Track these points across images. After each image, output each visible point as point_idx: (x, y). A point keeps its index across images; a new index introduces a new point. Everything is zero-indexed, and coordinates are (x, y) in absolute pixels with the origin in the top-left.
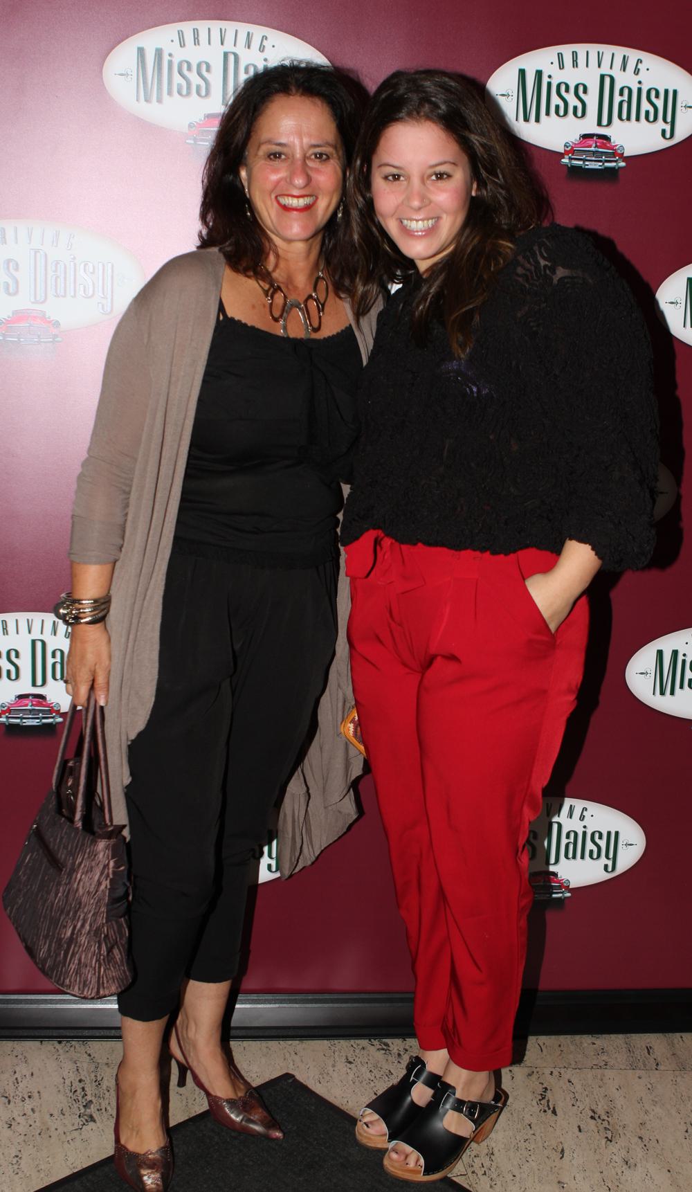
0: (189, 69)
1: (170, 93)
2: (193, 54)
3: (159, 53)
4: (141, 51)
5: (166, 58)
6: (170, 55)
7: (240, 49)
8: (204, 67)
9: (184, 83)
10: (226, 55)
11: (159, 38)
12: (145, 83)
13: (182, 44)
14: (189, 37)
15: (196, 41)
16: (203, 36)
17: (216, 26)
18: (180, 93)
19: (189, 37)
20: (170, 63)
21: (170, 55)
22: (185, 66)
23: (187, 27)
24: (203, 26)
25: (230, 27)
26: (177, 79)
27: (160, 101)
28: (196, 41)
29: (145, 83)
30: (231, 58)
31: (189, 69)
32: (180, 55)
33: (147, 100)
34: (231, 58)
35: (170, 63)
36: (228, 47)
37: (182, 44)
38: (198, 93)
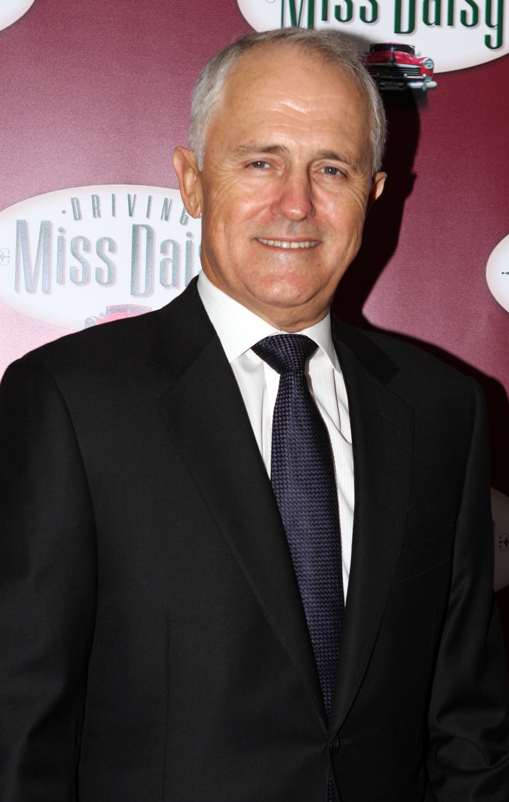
0: (87, 248)
1: (61, 281)
2: (92, 228)
3: (46, 229)
4: (22, 227)
5: (56, 234)
6: (61, 230)
7: (155, 221)
8: (106, 245)
9: (79, 267)
10: (136, 229)
11: (49, 209)
12: (27, 266)
13: (77, 217)
14: (86, 207)
15: (96, 212)
16: (105, 205)
17: (122, 192)
18: (74, 280)
19: (86, 207)
20: (61, 240)
21: (61, 230)
22: (81, 244)
23: (84, 194)
24: (105, 192)
25: (141, 193)
26: (70, 261)
27: (47, 291)
28: (96, 212)
29: (27, 266)
30: (143, 233)
31: (87, 248)
32: (74, 230)
33: (31, 290)
34: (143, 233)
35: (61, 240)
36: (140, 217)
37: (77, 217)
38: (99, 280)
